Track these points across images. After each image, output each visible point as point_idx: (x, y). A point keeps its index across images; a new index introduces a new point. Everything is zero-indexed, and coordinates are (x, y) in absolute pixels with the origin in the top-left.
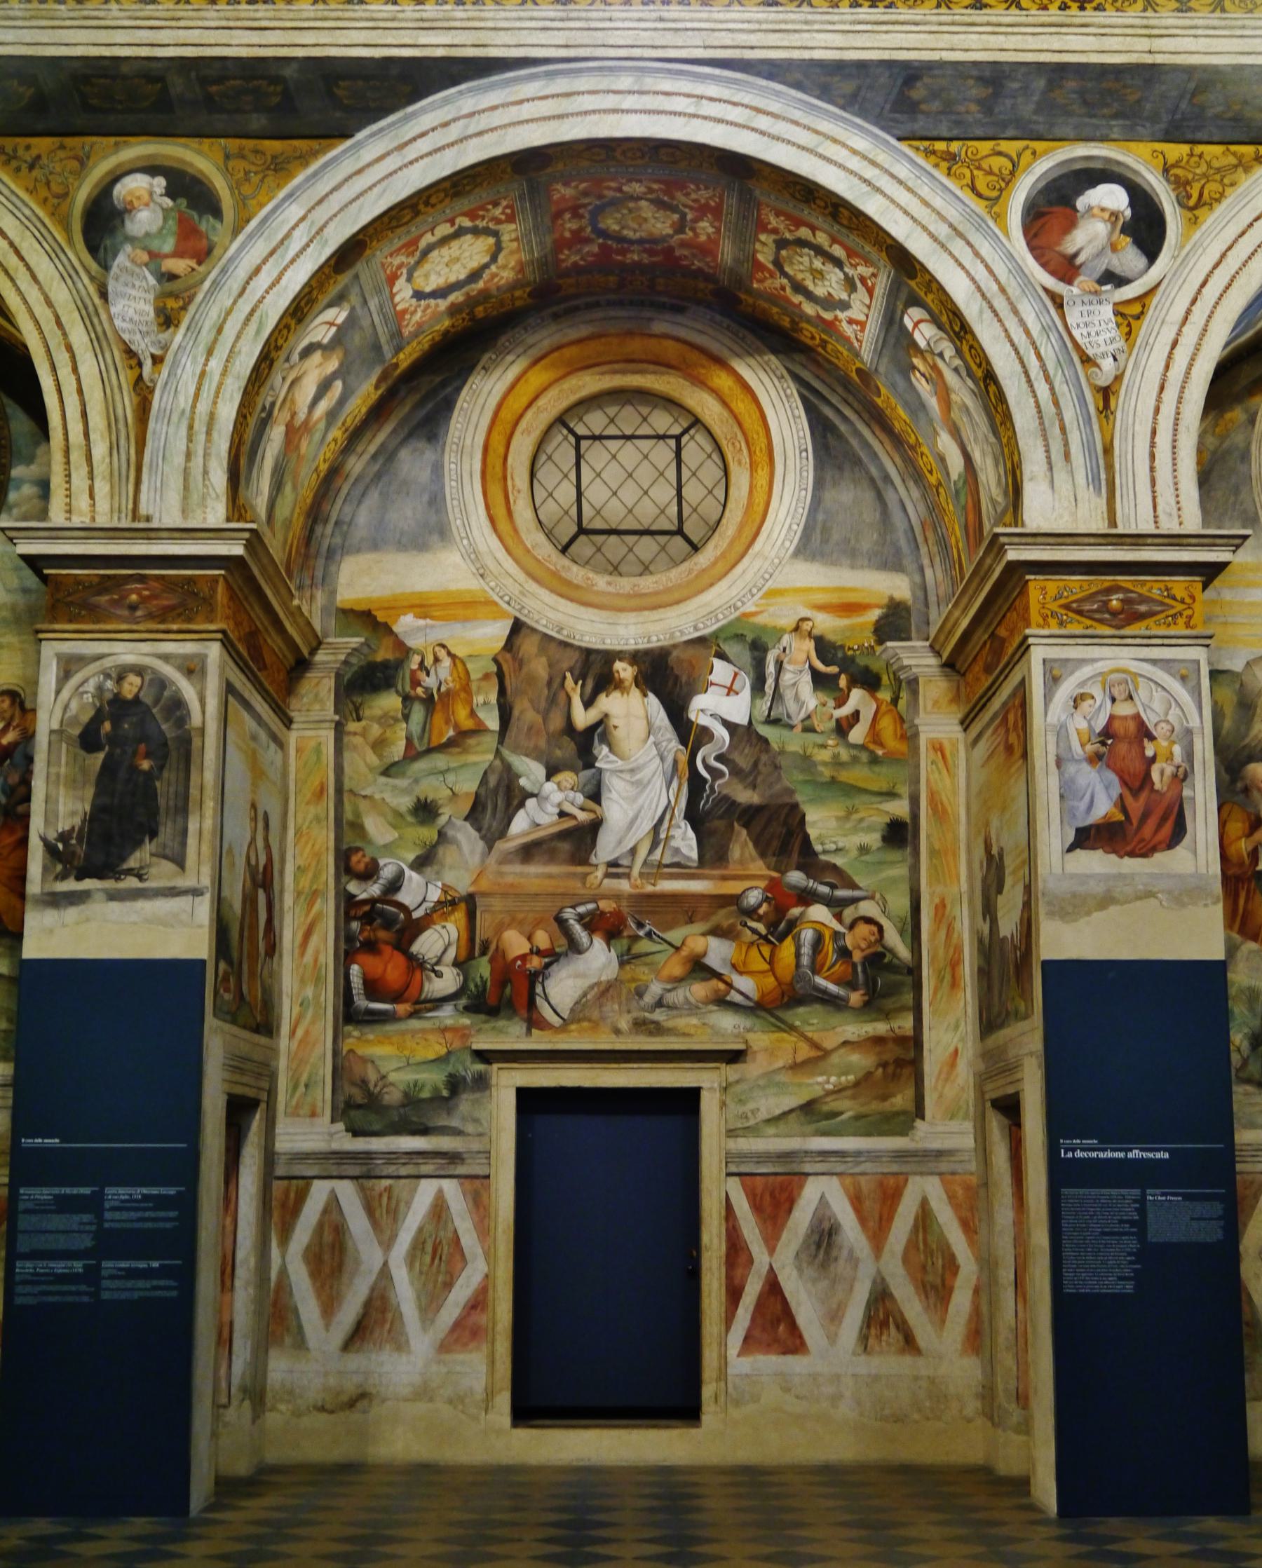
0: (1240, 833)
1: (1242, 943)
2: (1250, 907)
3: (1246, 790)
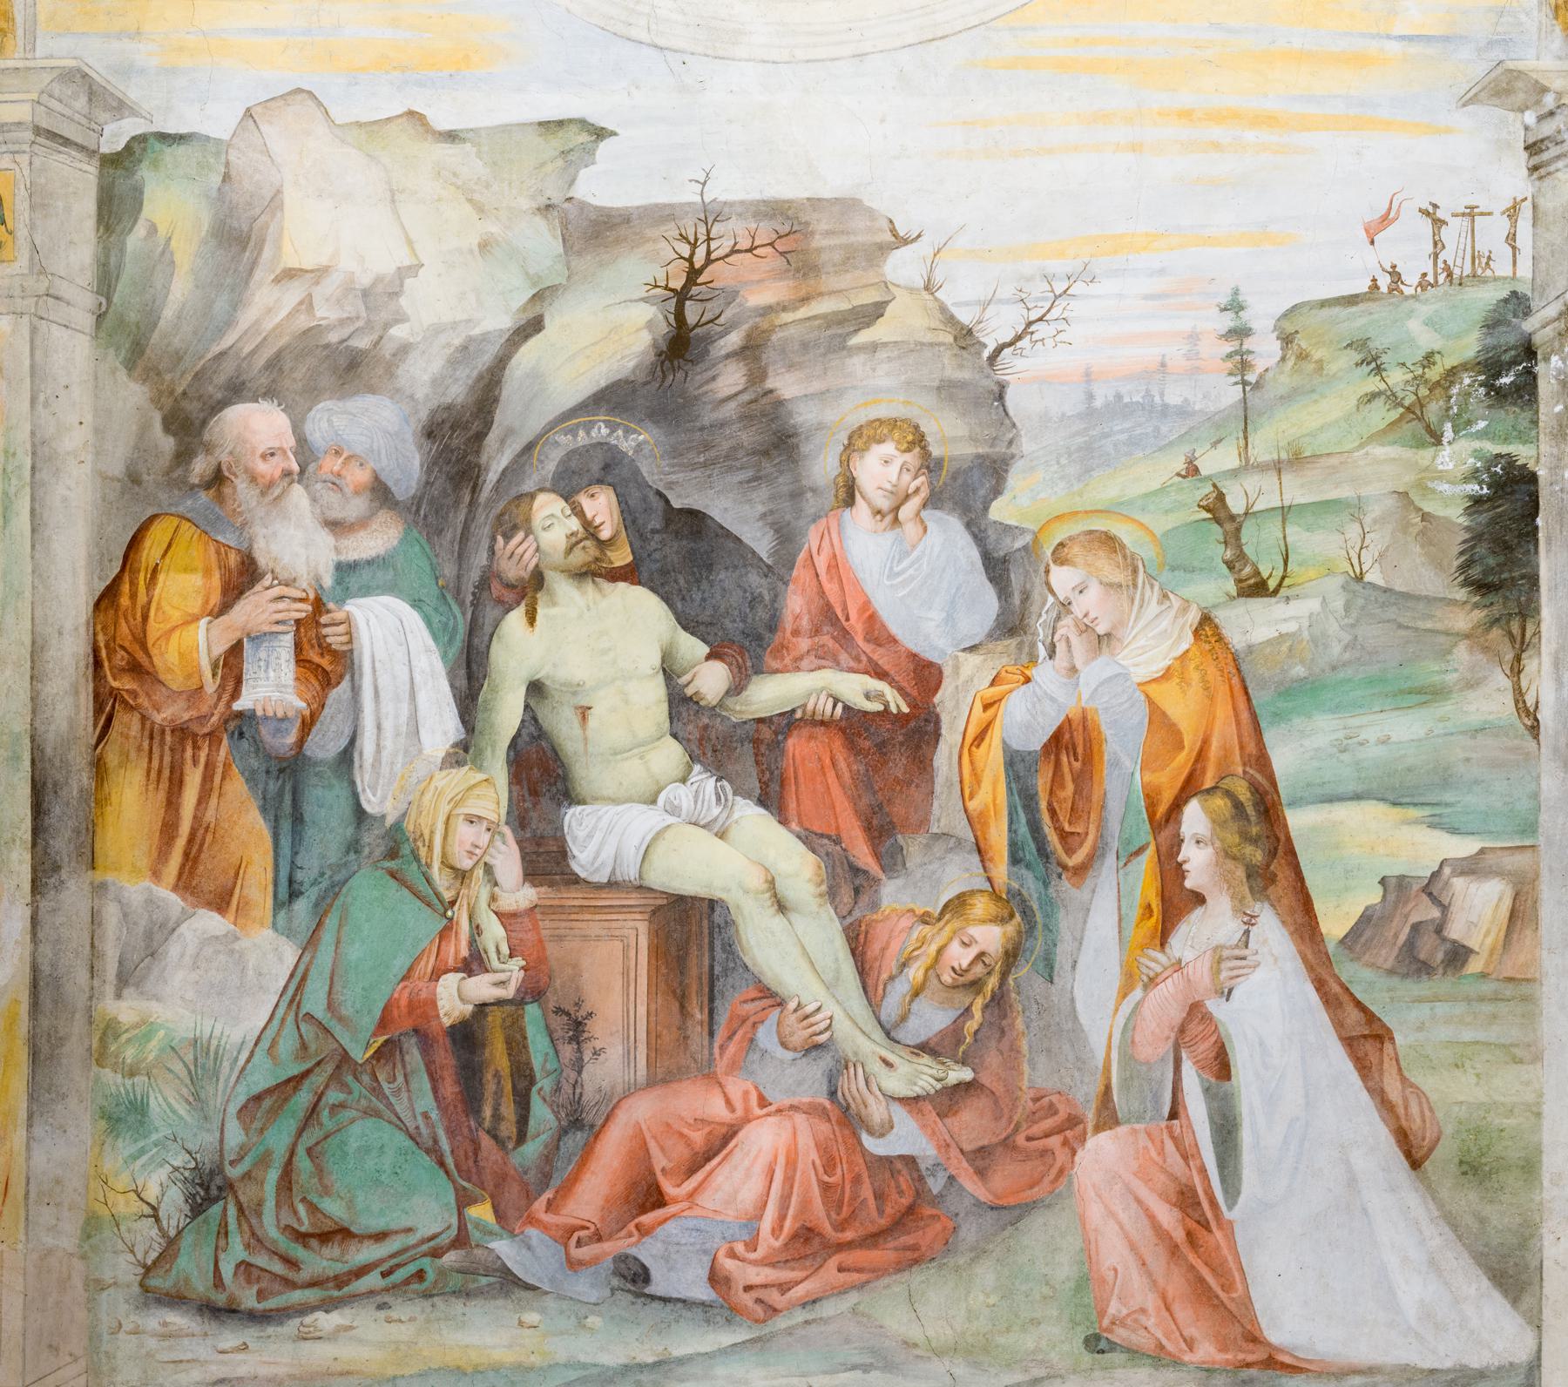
0: (195, 606)
1: (185, 917)
2: (210, 816)
3: (217, 480)
